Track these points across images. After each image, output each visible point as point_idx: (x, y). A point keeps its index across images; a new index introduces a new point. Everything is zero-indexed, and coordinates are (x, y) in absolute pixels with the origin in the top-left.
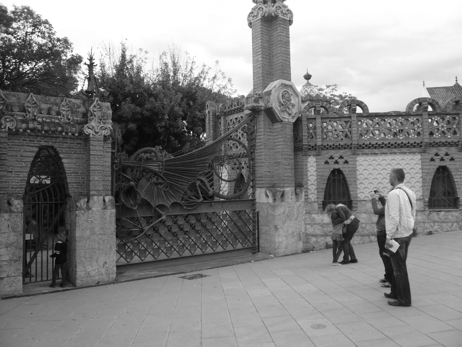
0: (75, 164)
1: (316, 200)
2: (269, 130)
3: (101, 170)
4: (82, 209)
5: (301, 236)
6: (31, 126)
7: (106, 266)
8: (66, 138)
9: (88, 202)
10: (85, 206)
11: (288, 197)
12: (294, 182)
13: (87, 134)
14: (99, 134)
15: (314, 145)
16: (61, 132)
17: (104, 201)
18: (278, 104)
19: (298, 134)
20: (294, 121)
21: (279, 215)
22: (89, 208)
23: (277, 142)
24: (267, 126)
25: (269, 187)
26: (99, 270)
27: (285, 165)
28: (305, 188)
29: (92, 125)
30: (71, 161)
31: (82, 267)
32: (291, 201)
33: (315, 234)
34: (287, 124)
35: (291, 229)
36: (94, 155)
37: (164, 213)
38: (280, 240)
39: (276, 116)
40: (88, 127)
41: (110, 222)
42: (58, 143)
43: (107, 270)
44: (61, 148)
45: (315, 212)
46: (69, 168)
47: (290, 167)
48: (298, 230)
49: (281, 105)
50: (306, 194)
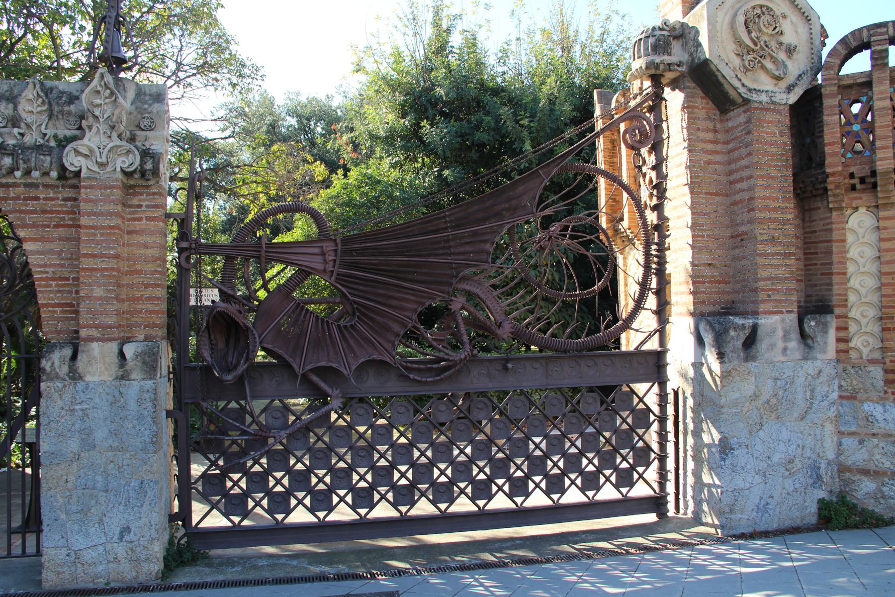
0: (59, 253)
1: (877, 355)
2: (710, 136)
3: (113, 269)
4: (57, 376)
5: (822, 471)
7: (127, 538)
8: (36, 186)
9: (74, 357)
10: (66, 369)
11: (772, 346)
12: (795, 298)
13: (72, 169)
14: (109, 169)
15: (866, 171)
16: (11, 171)
17: (122, 355)
18: (731, 46)
19: (813, 142)
20: (793, 98)
21: (735, 403)
22: (75, 376)
23: (736, 171)
24: (701, 124)
25: (710, 314)
26: (109, 547)
28: (838, 317)
29: (87, 146)
30: (49, 246)
31: (57, 537)
32: (783, 359)
33: (872, 467)
34: (767, 110)
35: (782, 447)
36: (92, 227)
37: (336, 392)
38: (739, 482)
39: (726, 86)
40: (75, 150)
41: (140, 418)
42: (13, 199)
43: (132, 549)
44: (21, 212)
45: (874, 395)
46: (41, 266)
47: (779, 248)
48: (808, 453)
49: (743, 50)
50: (842, 334)
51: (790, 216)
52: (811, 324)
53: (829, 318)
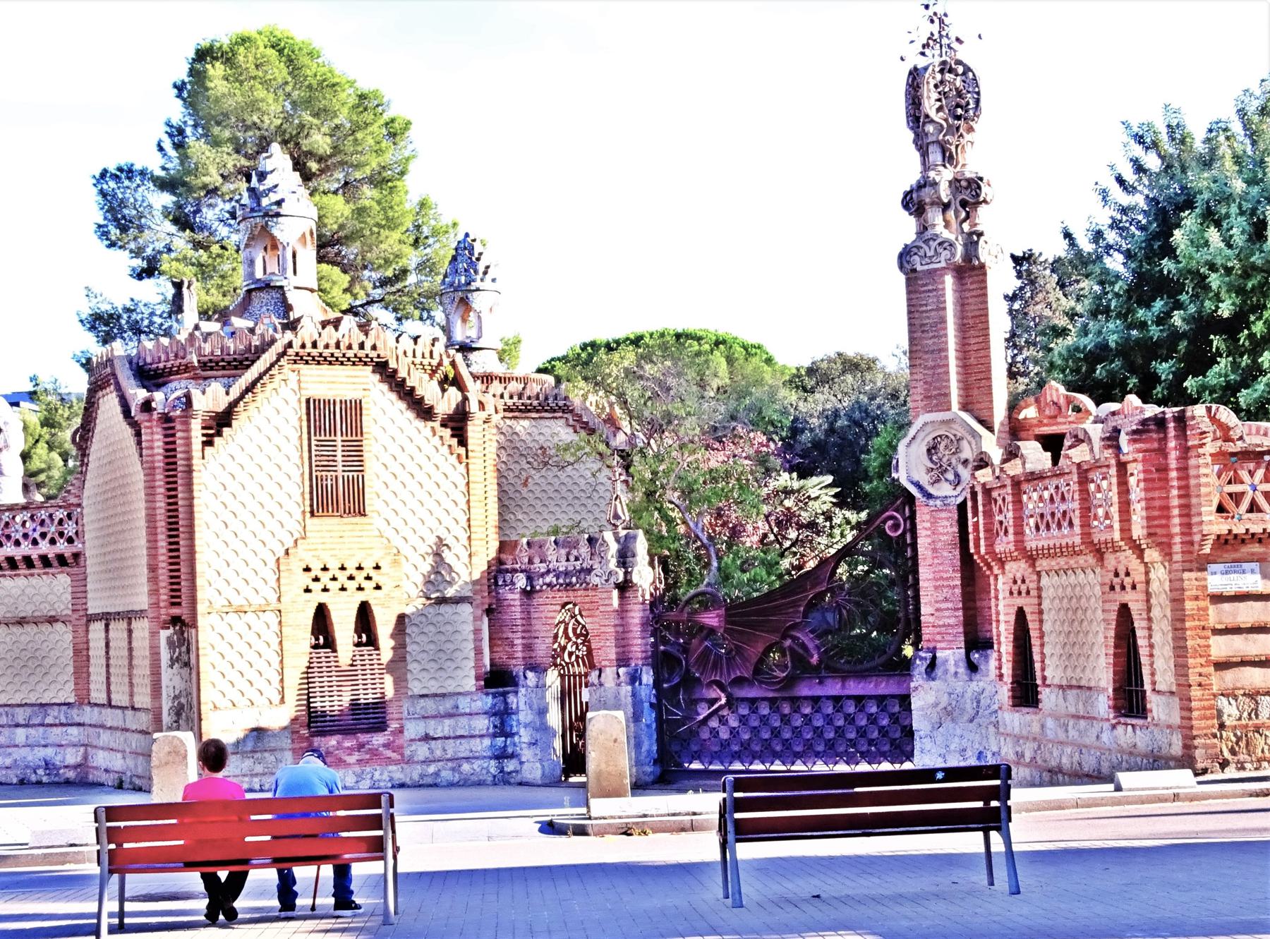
6: (548, 579)
9: (600, 676)
20: (960, 500)
27: (937, 602)
35: (957, 739)
47: (950, 605)
48: (977, 746)
51: (959, 583)
52: (975, 656)
53: (989, 652)
